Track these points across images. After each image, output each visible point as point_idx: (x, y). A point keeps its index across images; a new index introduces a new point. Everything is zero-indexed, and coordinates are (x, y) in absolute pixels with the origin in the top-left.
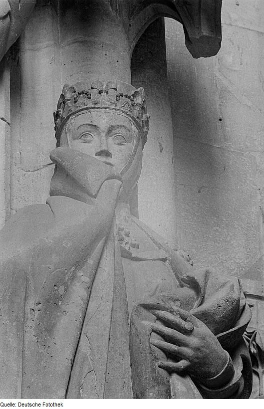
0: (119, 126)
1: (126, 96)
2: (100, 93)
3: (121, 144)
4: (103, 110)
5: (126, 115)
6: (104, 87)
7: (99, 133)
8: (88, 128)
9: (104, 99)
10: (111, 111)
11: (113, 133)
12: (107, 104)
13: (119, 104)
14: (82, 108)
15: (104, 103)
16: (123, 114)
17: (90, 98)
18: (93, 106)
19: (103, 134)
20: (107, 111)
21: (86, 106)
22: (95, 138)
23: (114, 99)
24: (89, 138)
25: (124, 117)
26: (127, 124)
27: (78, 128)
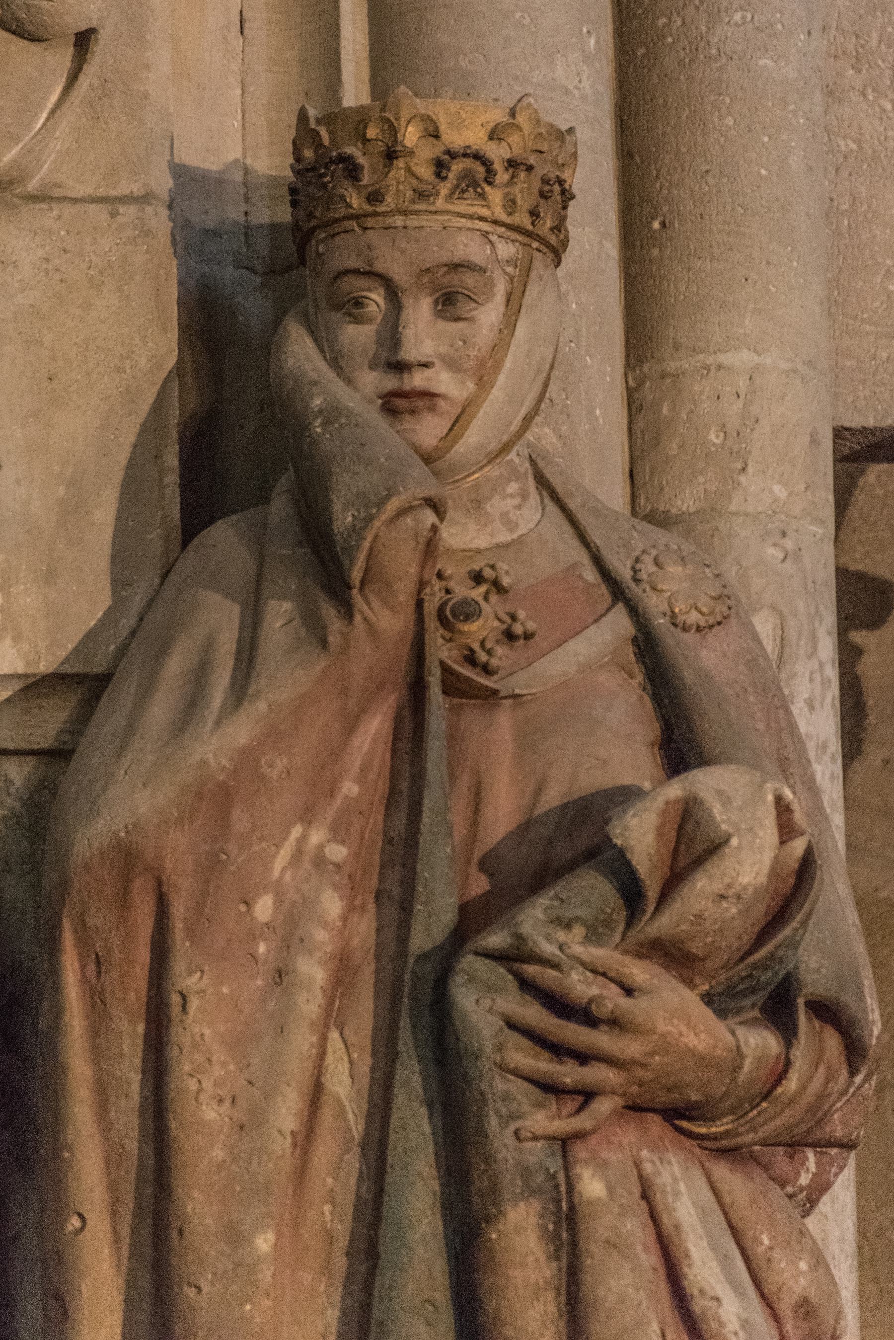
4: (399, 221)
8: (362, 282)
20: (413, 221)
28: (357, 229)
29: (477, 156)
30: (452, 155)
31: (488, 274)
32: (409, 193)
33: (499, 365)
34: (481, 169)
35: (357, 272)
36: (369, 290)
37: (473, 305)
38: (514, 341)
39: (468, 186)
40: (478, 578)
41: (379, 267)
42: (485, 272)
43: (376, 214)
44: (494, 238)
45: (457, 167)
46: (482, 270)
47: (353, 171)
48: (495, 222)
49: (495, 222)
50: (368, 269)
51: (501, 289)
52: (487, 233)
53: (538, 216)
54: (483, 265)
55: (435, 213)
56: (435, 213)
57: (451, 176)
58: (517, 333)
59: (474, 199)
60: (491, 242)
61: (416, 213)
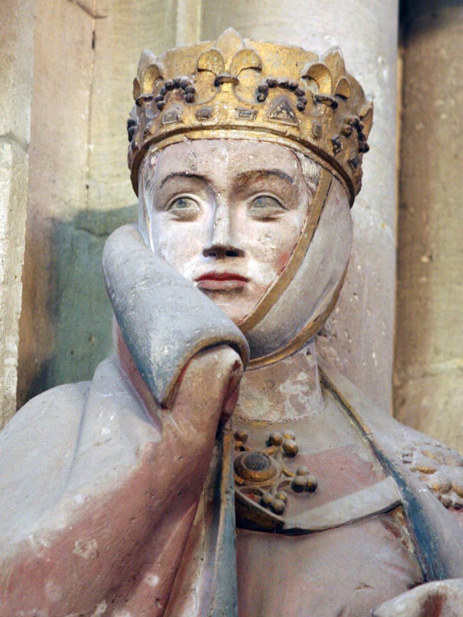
0: (265, 174)
1: (284, 86)
2: (218, 82)
3: (267, 219)
4: (222, 133)
5: (281, 140)
6: (227, 67)
7: (213, 195)
8: (186, 184)
9: (225, 104)
10: (243, 134)
11: (250, 192)
12: (231, 116)
13: (262, 112)
14: (173, 127)
15: (226, 113)
16: (274, 138)
17: (190, 101)
18: (197, 123)
19: (223, 199)
20: (232, 134)
21: (181, 125)
22: (206, 206)
23: (249, 97)
24: (192, 208)
25: (276, 147)
26: (286, 165)
27: (164, 182)
28: (185, 139)
29: (293, 88)
30: (273, 85)
31: (294, 183)
32: (232, 112)
33: (298, 261)
34: (293, 98)
35: (183, 175)
36: (190, 192)
37: (281, 209)
38: (311, 245)
39: (282, 109)
40: (271, 442)
41: (200, 171)
42: (292, 182)
43: (202, 128)
44: (301, 156)
45: (273, 94)
46: (290, 180)
47: (189, 97)
48: (303, 143)
49: (303, 143)
50: (192, 172)
51: (305, 199)
52: (296, 150)
53: (339, 146)
54: (290, 174)
55: (253, 128)
56: (253, 128)
57: (268, 100)
58: (314, 239)
59: (285, 120)
60: (298, 159)
61: (237, 127)
